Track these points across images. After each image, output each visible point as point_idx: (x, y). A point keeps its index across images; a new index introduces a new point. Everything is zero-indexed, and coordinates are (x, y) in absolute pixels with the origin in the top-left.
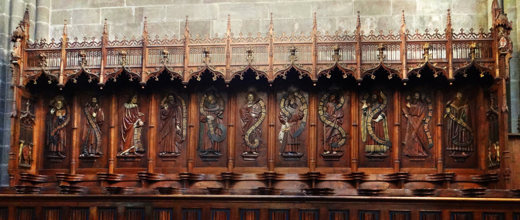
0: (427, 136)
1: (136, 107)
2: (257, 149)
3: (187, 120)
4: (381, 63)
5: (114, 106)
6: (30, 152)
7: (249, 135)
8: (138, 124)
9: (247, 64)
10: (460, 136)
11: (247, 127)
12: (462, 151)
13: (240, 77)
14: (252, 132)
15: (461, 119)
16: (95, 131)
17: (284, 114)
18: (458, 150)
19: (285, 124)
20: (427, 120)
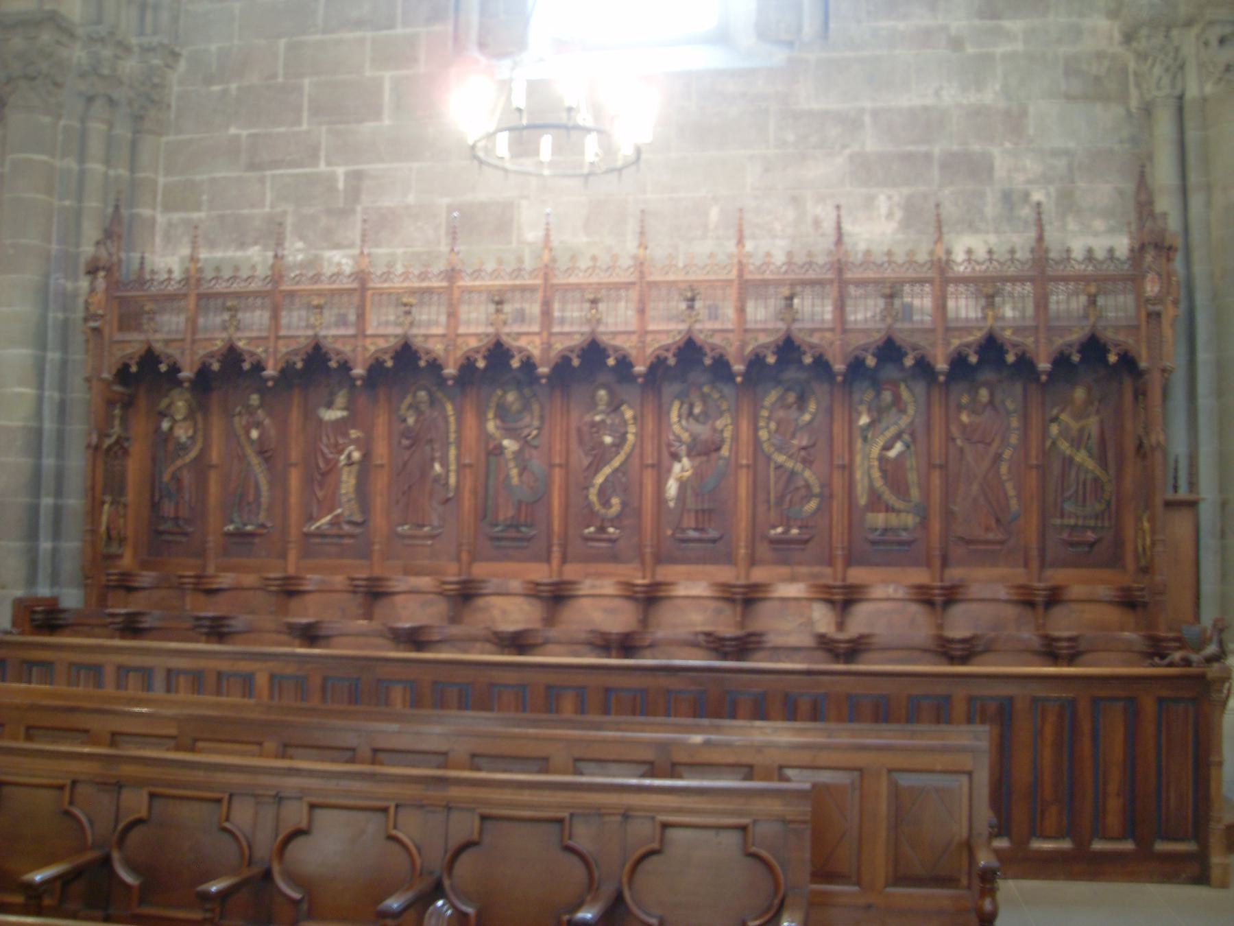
0: (1005, 494)
2: (617, 521)
3: (458, 448)
5: (295, 416)
8: (349, 456)
10: (1081, 492)
11: (595, 467)
14: (606, 480)
18: (1076, 526)
19: (680, 461)
20: (1007, 454)
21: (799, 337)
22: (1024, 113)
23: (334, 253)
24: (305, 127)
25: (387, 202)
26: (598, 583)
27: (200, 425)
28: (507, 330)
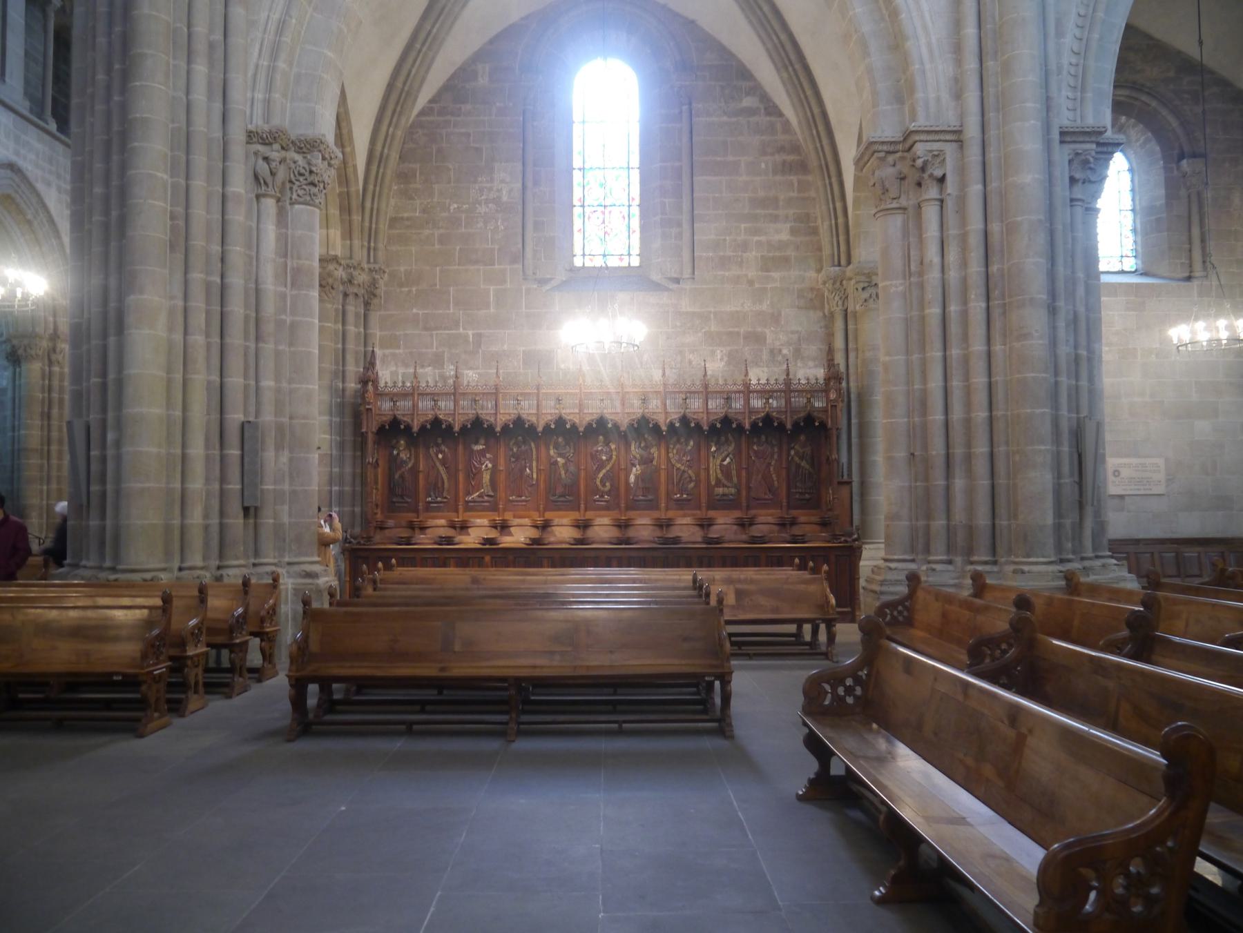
1: (483, 449)
2: (609, 493)
3: (537, 461)
4: (726, 412)
8: (486, 466)
9: (599, 411)
12: (806, 493)
14: (604, 475)
15: (804, 461)
19: (635, 467)
20: (773, 463)
21: (689, 415)
22: (780, 314)
23: (468, 371)
24: (451, 311)
25: (494, 349)
26: (602, 519)
27: (413, 452)
28: (564, 411)
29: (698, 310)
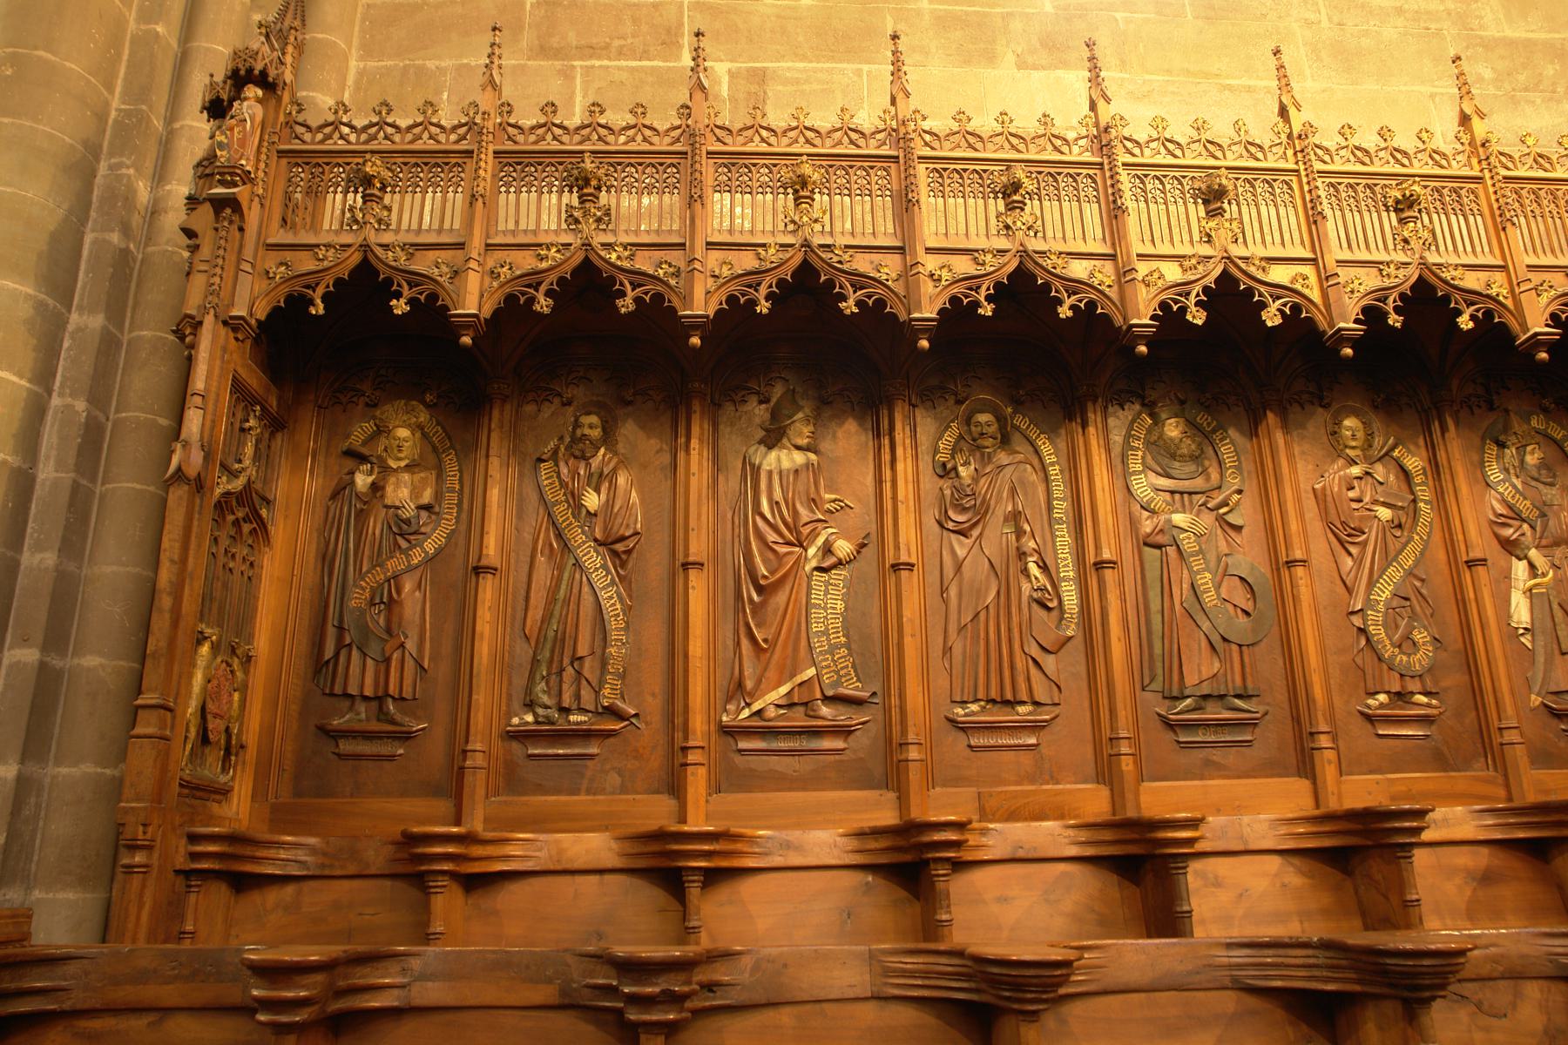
1: (808, 465)
2: (1430, 682)
6: (236, 696)
7: (1381, 607)
8: (827, 550)
13: (1385, 315)
16: (598, 585)
17: (1510, 507)
29: (1543, 36)
